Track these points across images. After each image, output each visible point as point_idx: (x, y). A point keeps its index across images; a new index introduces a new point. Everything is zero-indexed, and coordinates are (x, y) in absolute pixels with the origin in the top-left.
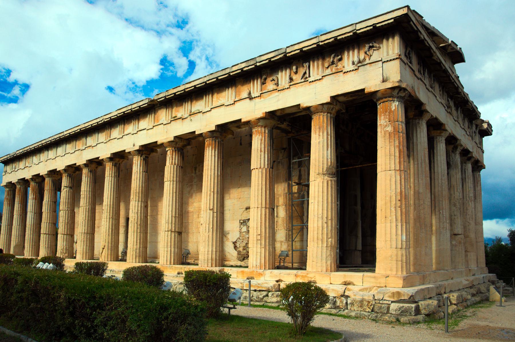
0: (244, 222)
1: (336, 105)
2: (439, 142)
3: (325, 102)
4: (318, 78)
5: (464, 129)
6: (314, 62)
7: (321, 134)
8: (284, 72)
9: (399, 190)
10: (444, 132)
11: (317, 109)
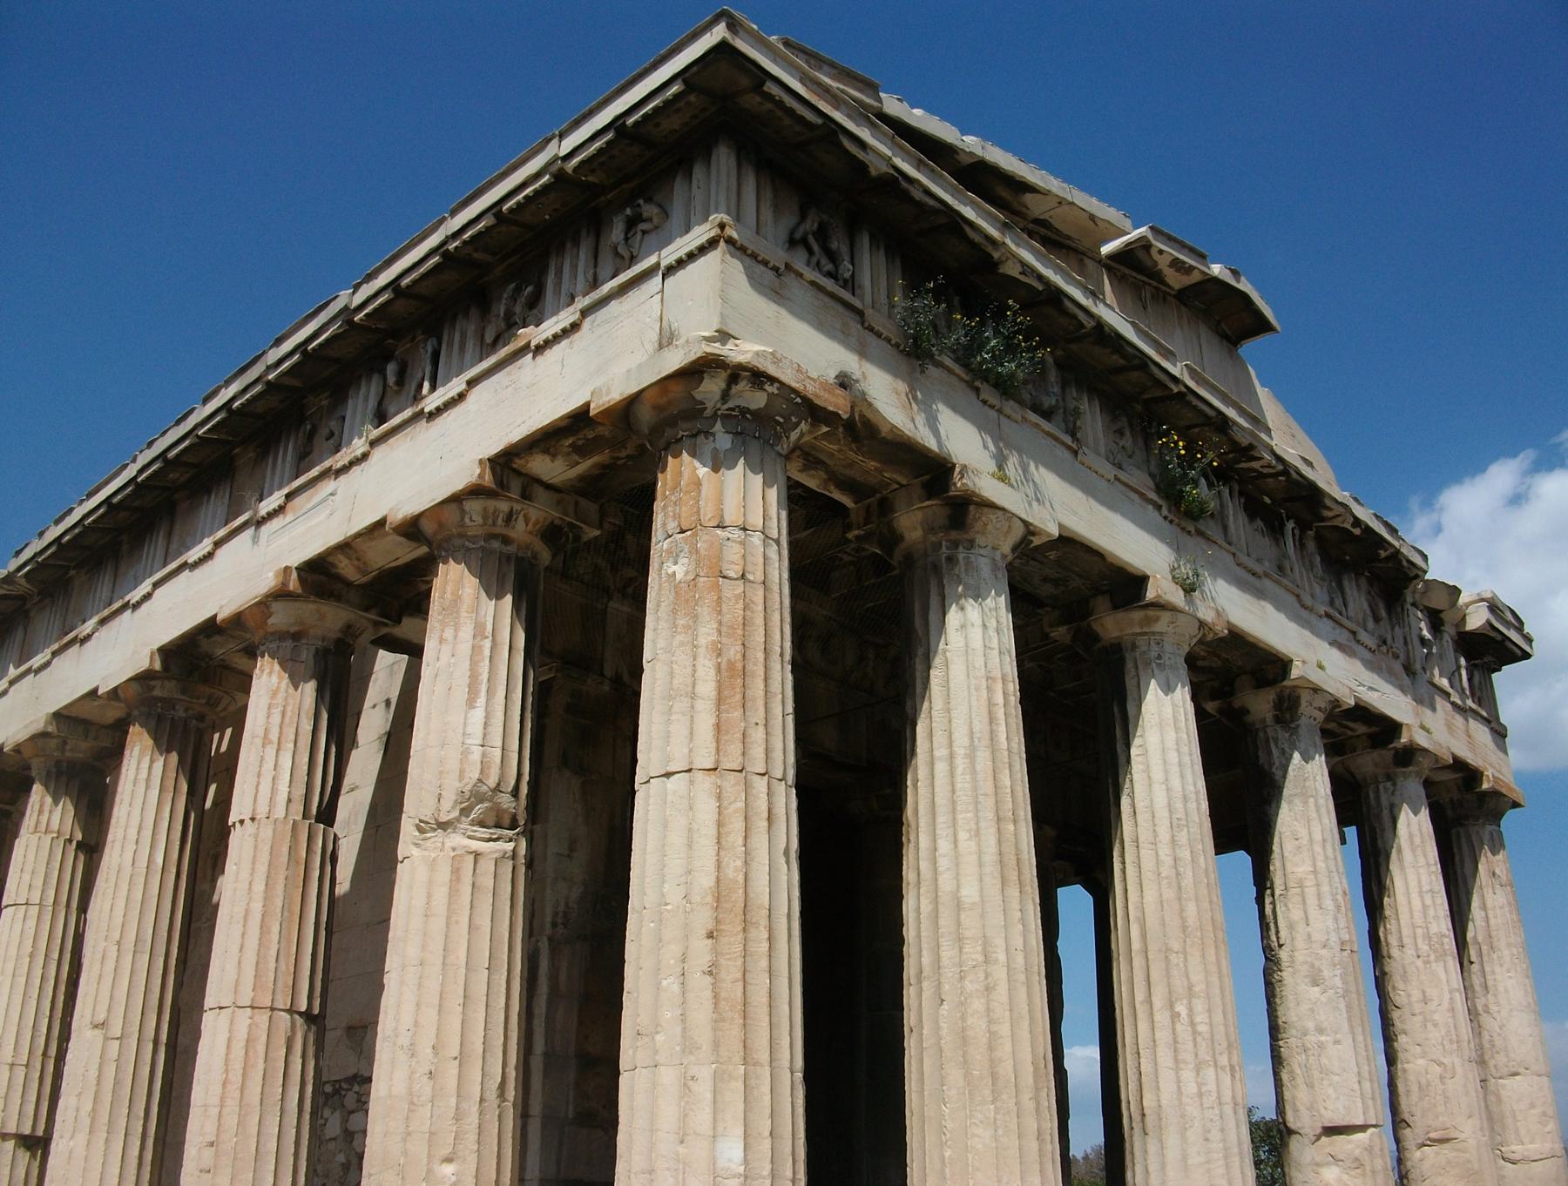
0: (336, 1092)
1: (526, 495)
2: (1148, 664)
3: (458, 485)
5: (1328, 616)
6: (453, 326)
7: (449, 633)
8: (363, 389)
9: (705, 880)
10: (1166, 617)
11: (441, 525)
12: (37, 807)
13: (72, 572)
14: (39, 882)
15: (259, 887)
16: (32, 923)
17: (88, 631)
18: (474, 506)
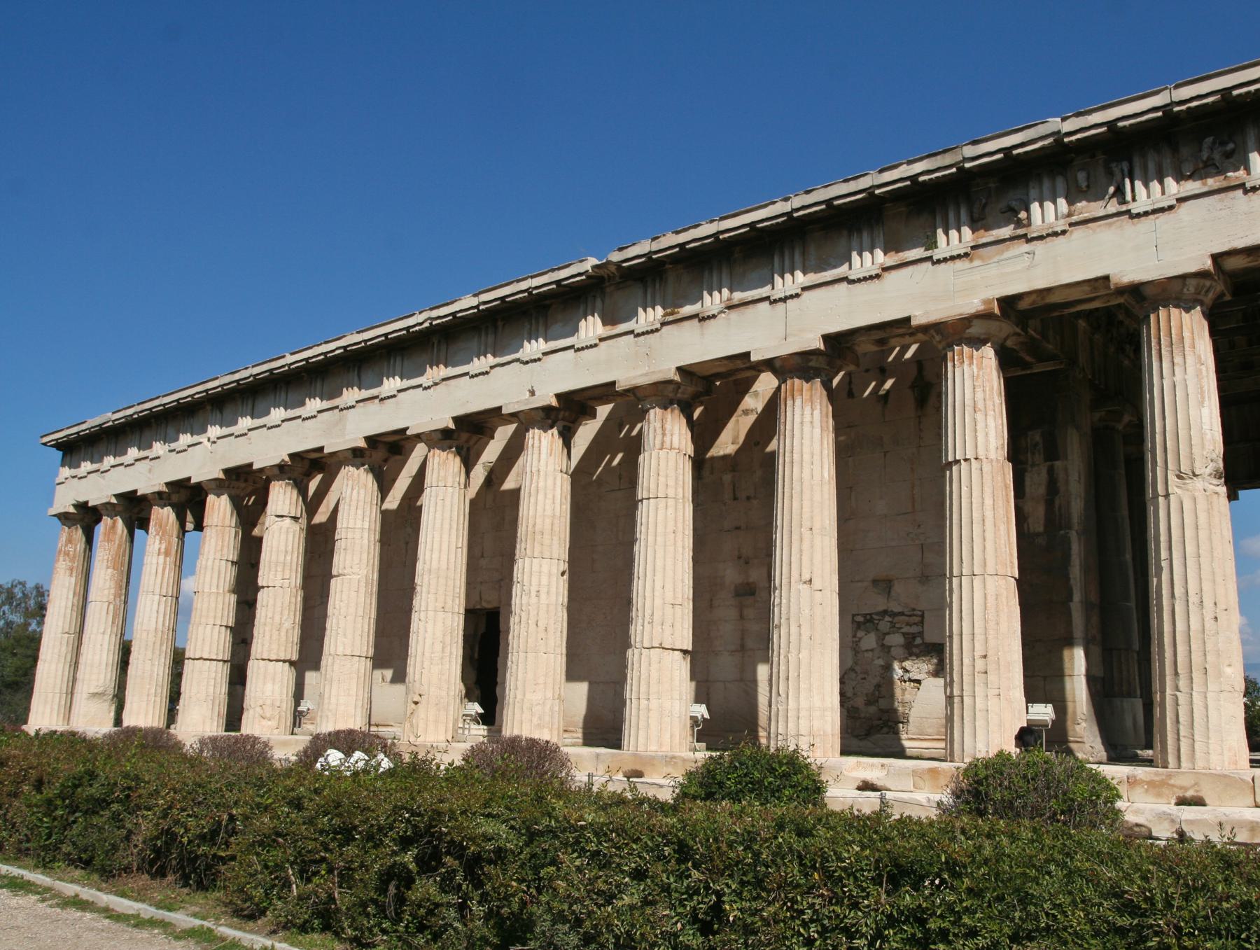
3: (1193, 268)
4: (1165, 204)
12: (659, 431)
13: (668, 266)
14: (671, 483)
15: (988, 502)
16: (671, 510)
17: (715, 312)
18: (1192, 283)
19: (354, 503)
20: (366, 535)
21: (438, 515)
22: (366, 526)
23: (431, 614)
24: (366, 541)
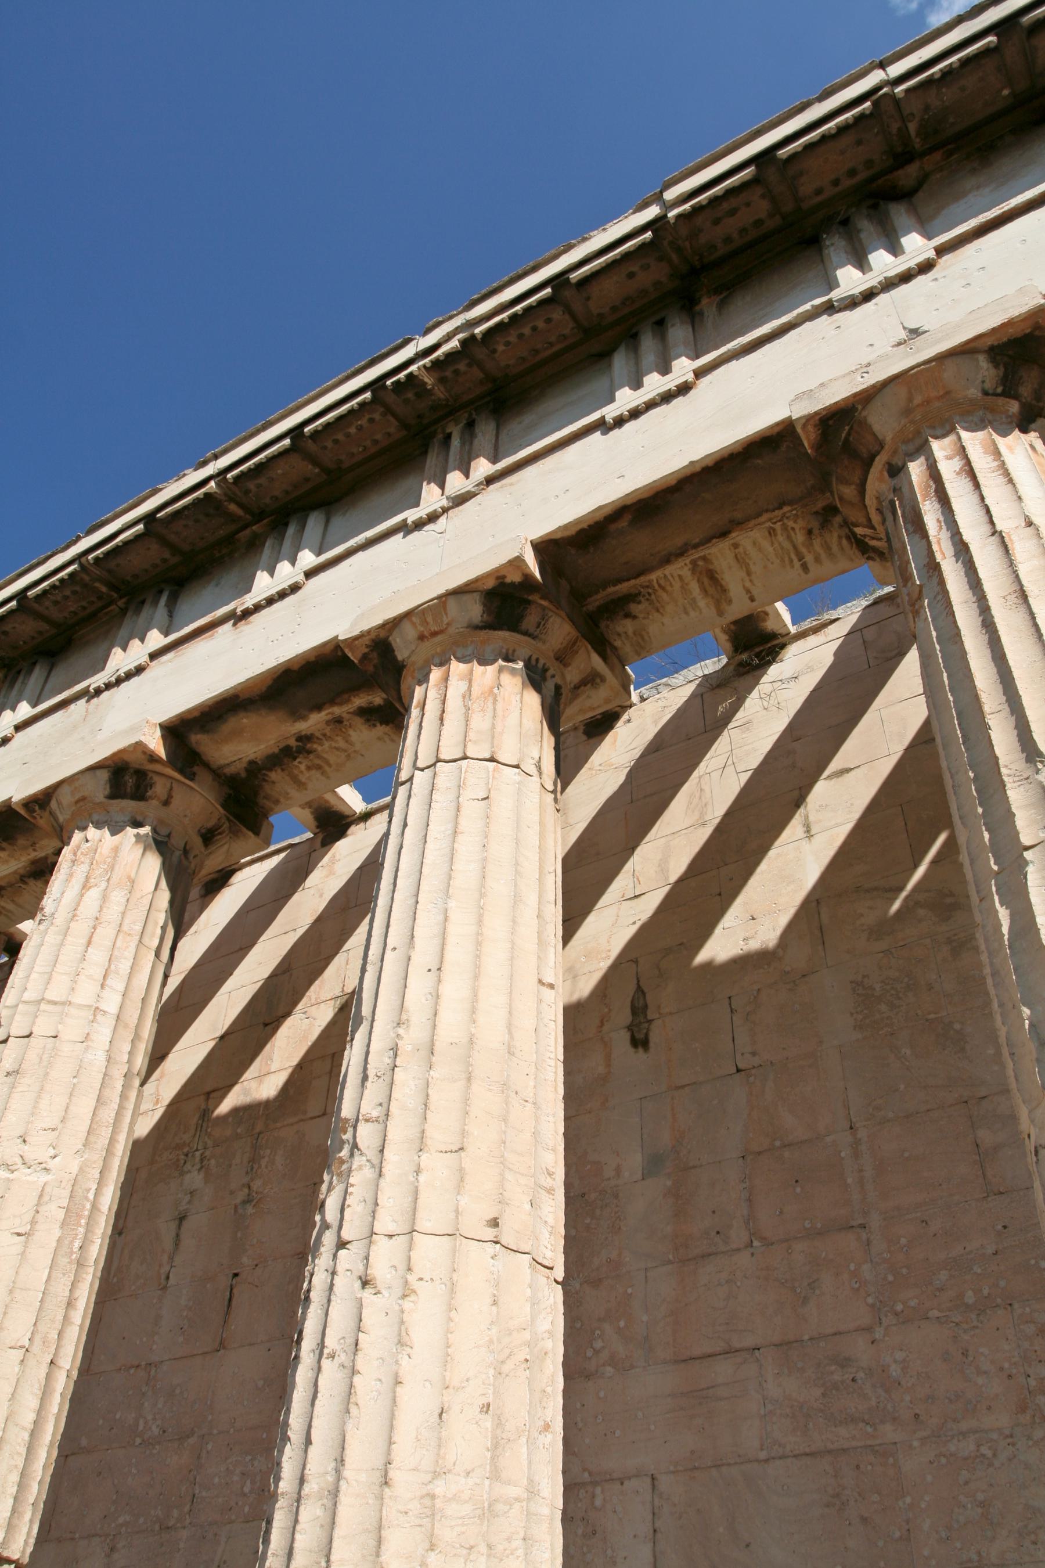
19: (80, 928)
20: (103, 1032)
21: (467, 846)
22: (111, 1003)
23: (429, 1252)
24: (98, 1057)
